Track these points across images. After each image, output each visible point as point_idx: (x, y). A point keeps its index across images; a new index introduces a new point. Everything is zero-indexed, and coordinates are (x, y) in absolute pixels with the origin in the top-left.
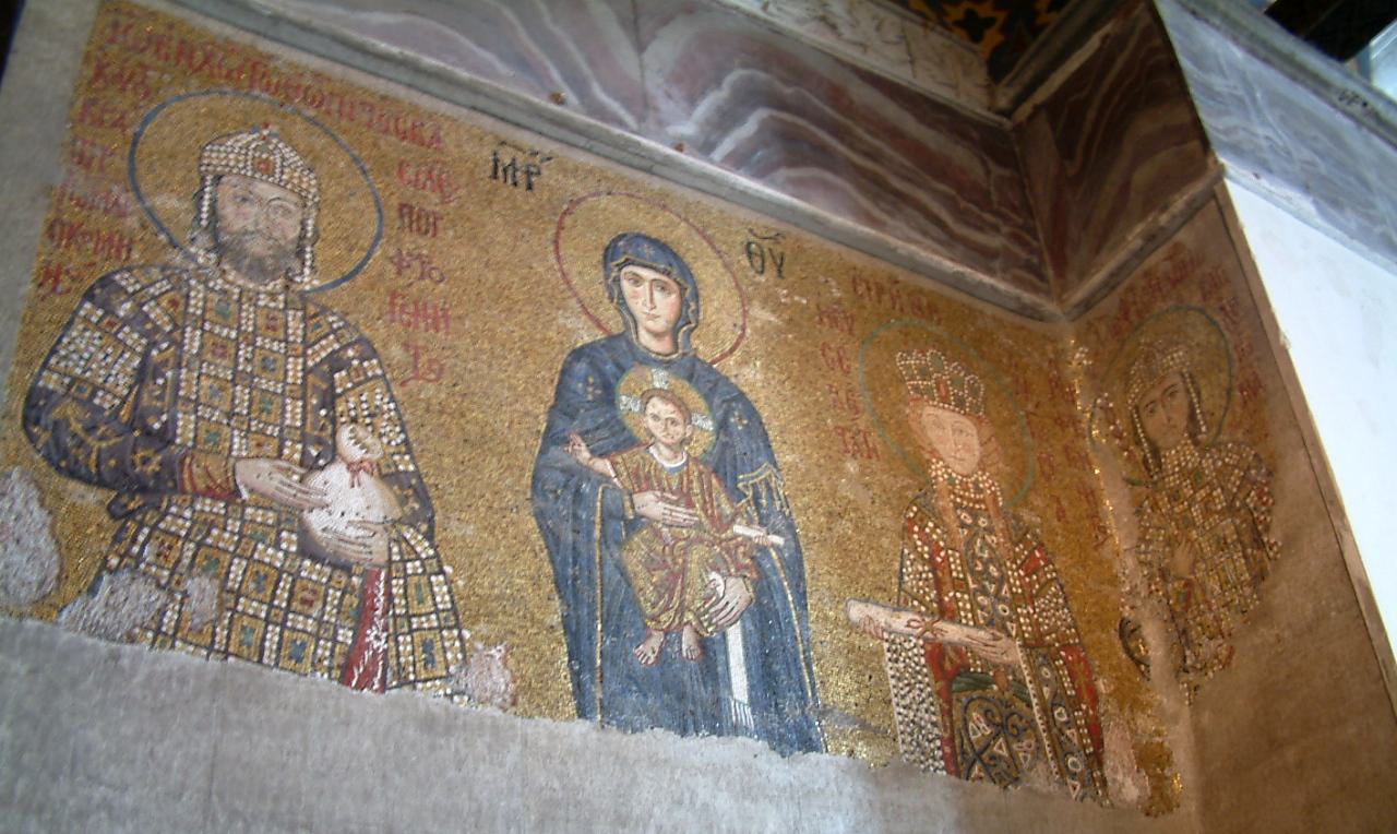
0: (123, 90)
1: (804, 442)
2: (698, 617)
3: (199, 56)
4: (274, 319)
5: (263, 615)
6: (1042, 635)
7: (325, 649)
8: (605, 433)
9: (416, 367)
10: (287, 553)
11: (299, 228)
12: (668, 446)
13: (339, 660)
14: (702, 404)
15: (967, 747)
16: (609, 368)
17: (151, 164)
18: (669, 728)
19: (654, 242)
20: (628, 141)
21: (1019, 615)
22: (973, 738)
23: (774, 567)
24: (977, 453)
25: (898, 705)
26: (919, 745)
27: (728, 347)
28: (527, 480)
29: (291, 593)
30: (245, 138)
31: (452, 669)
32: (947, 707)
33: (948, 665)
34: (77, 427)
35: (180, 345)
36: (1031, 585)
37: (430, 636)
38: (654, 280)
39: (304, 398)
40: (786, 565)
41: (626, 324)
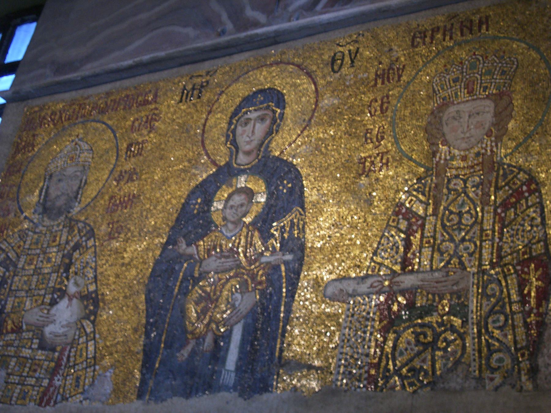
5: (17, 381)
12: (233, 223)
13: (40, 395)
15: (391, 367)
18: (182, 395)
20: (251, 37)
23: (281, 276)
24: (487, 126)
29: (30, 368)
31: (86, 387)
35: (15, 266)
37: (80, 373)
38: (259, 117)
39: (58, 272)
41: (231, 156)
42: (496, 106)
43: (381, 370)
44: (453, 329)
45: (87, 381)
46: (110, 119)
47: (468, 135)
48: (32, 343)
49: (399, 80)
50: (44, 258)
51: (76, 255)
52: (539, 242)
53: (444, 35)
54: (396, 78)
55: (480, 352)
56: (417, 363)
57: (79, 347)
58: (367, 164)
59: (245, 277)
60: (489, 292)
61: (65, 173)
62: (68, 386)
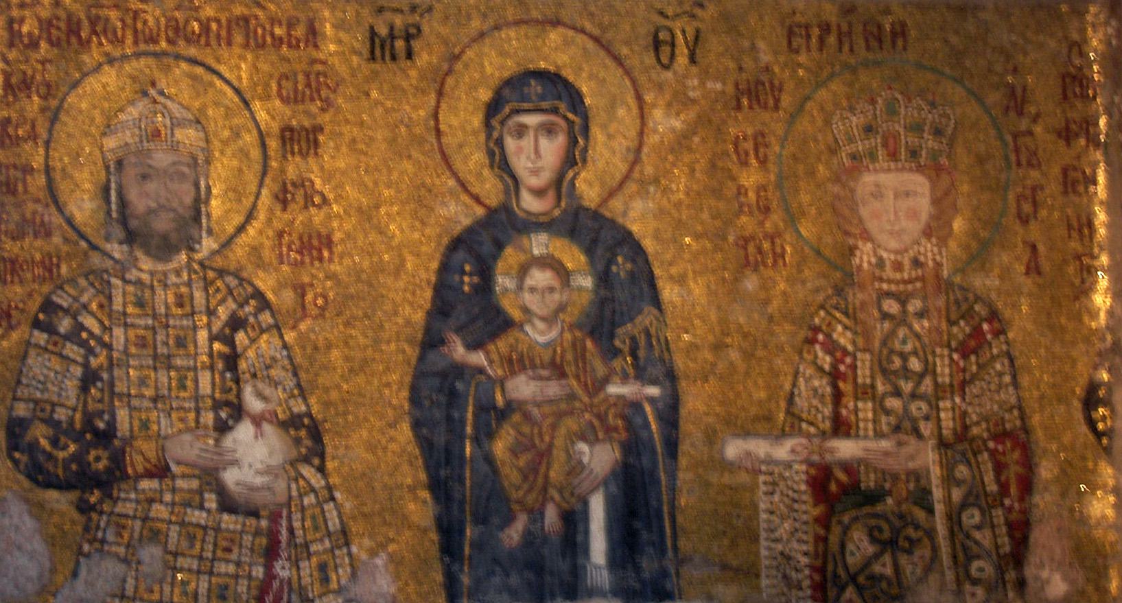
0: (29, 97)
1: (694, 272)
2: (561, 492)
3: (85, 23)
4: (181, 296)
5: (195, 567)
6: (966, 428)
7: (242, 585)
8: (480, 323)
9: (303, 307)
10: (209, 511)
11: (193, 189)
12: (543, 319)
14: (583, 258)
15: (841, 572)
16: (487, 248)
17: (63, 170)
19: (540, 75)
21: (938, 409)
22: (850, 560)
24: (924, 217)
25: (767, 539)
26: (785, 577)
27: (618, 177)
28: (405, 394)
29: (215, 545)
30: (133, 112)
31: (343, 582)
32: (822, 532)
33: (833, 487)
34: (44, 442)
35: (109, 347)
36: (964, 370)
40: (660, 417)
41: (507, 192)
42: (933, 188)
43: (829, 575)
44: (917, 527)
45: (340, 571)
46: (218, 61)
47: (896, 228)
48: (202, 500)
49: (776, 108)
50: (168, 335)
51: (241, 337)
52: (1010, 410)
53: (840, 42)
54: (771, 102)
55: (955, 557)
56: (877, 568)
57: (309, 513)
58: (751, 249)
59: (587, 416)
60: (958, 475)
61: (150, 162)
62: (306, 580)
